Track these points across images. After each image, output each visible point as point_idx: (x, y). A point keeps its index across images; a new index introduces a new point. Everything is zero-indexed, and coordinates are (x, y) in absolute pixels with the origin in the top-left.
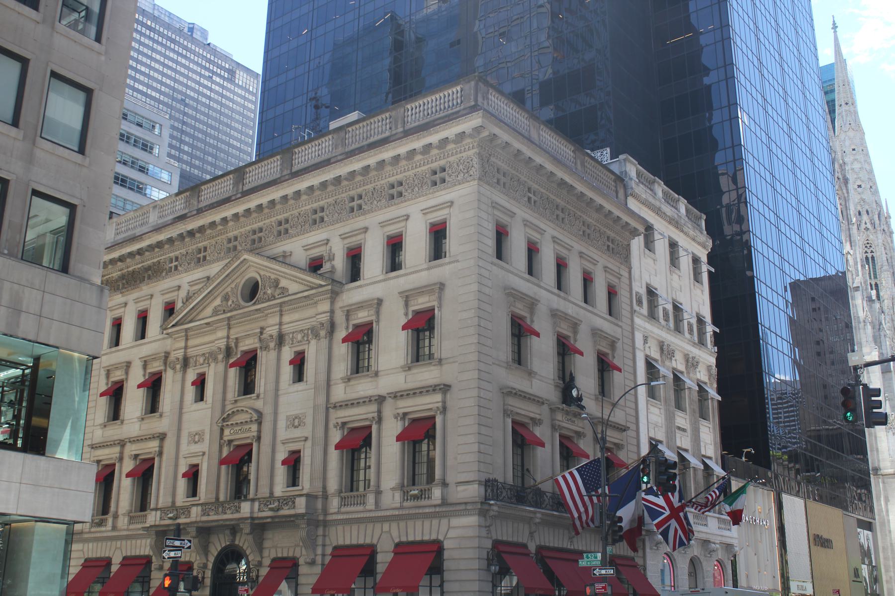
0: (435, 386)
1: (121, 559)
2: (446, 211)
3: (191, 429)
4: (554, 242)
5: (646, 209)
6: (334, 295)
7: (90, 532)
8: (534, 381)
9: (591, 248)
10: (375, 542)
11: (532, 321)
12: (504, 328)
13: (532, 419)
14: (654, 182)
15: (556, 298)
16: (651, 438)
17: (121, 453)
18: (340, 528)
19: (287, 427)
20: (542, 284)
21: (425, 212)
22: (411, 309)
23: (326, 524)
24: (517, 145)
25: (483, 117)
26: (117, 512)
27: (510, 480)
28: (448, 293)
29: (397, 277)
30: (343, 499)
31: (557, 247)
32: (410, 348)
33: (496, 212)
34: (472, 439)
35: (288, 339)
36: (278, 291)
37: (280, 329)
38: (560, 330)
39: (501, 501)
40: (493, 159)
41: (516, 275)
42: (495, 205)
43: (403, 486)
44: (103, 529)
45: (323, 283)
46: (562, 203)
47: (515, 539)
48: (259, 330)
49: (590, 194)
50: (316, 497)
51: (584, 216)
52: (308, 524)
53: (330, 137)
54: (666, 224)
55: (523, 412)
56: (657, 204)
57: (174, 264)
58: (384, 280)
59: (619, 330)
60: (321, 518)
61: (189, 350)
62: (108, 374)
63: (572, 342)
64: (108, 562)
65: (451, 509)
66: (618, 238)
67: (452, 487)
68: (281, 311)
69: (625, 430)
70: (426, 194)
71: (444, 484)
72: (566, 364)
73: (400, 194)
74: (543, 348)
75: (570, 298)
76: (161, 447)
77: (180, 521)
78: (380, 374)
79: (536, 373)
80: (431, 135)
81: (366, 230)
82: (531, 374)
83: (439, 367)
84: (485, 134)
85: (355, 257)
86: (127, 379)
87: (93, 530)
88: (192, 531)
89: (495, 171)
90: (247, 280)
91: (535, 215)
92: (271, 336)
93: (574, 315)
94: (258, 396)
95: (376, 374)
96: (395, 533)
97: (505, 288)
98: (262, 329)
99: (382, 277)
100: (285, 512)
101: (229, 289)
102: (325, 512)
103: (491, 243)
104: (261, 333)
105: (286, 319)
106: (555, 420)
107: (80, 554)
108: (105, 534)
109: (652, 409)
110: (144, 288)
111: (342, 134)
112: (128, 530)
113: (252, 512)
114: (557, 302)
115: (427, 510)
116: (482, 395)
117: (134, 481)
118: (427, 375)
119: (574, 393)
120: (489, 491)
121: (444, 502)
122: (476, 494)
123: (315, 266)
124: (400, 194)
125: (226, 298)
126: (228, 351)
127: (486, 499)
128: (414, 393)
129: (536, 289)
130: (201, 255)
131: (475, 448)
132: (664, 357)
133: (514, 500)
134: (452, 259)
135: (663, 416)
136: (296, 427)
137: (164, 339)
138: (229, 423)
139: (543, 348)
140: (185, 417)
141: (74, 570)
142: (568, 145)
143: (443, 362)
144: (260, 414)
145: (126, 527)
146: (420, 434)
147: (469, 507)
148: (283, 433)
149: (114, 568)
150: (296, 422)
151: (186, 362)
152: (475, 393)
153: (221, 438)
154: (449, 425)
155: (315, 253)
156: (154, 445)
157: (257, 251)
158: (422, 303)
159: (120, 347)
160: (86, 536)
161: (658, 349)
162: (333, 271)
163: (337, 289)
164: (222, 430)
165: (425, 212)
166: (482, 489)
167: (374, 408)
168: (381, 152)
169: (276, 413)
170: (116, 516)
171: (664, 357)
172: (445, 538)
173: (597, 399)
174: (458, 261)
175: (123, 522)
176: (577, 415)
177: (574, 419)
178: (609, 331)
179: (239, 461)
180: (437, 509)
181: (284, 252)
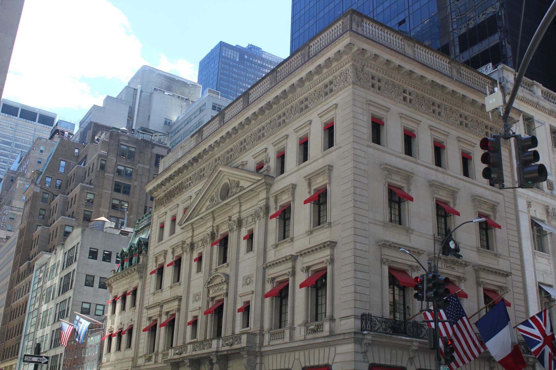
0: (324, 243)
2: (333, 112)
3: (193, 292)
4: (431, 129)
5: (525, 105)
6: (269, 186)
7: (144, 365)
8: (413, 237)
9: (468, 134)
10: (290, 367)
11: (409, 190)
12: (382, 196)
13: (410, 266)
14: (533, 85)
15: (434, 172)
16: (539, 283)
17: (161, 311)
18: (270, 357)
19: (243, 285)
20: (419, 161)
21: (320, 116)
22: (313, 188)
23: (262, 355)
24: (385, 55)
25: (350, 36)
27: (387, 314)
28: (335, 173)
29: (305, 166)
30: (272, 335)
31: (433, 133)
32: (312, 217)
33: (371, 108)
34: (350, 282)
35: (244, 222)
36: (239, 189)
37: (239, 216)
38: (439, 197)
39: (375, 331)
40: (367, 69)
41: (392, 155)
42: (370, 103)
43: (307, 322)
45: (260, 178)
46: (438, 101)
47: (393, 363)
48: (228, 218)
49: (461, 91)
50: (255, 334)
51: (461, 110)
52: (248, 355)
53: (268, 78)
54: (547, 116)
55: (399, 261)
56: (536, 100)
57: (189, 182)
58: (297, 170)
59: (501, 197)
60: (257, 350)
61: (194, 238)
63: (452, 206)
65: (335, 339)
66: (496, 126)
67: (337, 321)
68: (240, 203)
69: (507, 276)
70: (321, 103)
71: (332, 319)
72: (448, 224)
73: (307, 107)
74: (421, 212)
75: (448, 172)
76: (179, 305)
77: (182, 355)
78: (294, 239)
79: (413, 230)
80: (320, 58)
81: (287, 136)
82: (409, 231)
83: (329, 229)
84: (355, 49)
85: (281, 157)
88: (187, 362)
89: (368, 78)
90: (223, 185)
91: (412, 109)
92: (234, 221)
93: (453, 185)
94: (228, 265)
95: (292, 240)
96: (302, 360)
97: (381, 165)
98: (230, 217)
99: (296, 169)
100: (236, 346)
101: (214, 193)
102: (261, 345)
103: (366, 131)
104: (230, 220)
105: (243, 208)
106: (480, 278)
109: (540, 259)
110: (175, 201)
111: (275, 74)
113: (218, 347)
114: (436, 175)
115: (320, 341)
116: (358, 247)
118: (323, 235)
119: (452, 245)
120: (364, 323)
121: (332, 333)
122: (353, 327)
123: (260, 167)
124: (307, 107)
125: (212, 200)
126: (213, 235)
127: (362, 330)
128: (312, 251)
129: (413, 165)
130: (202, 174)
131: (352, 289)
132: (550, 218)
133: (389, 330)
134: (337, 147)
135: (552, 266)
136: (248, 284)
137: (183, 232)
138: (213, 284)
139: (421, 212)
140: (192, 284)
142: (443, 58)
143: (332, 225)
144: (227, 276)
146: (318, 283)
147: (347, 337)
148: (241, 290)
150: (247, 281)
151: (192, 246)
152: (352, 246)
153: (208, 296)
154: (336, 273)
155: (259, 159)
156: (175, 304)
157: (229, 165)
158: (319, 183)
159: (163, 241)
161: (544, 212)
162: (268, 170)
163: (269, 181)
164: (209, 291)
165: (320, 116)
166: (359, 322)
167: (289, 265)
168: (291, 79)
169: (237, 276)
170: (157, 355)
171: (550, 218)
172: (333, 363)
173: (478, 251)
174: (341, 147)
176: (453, 262)
177: (454, 266)
178: (490, 198)
179: (218, 311)
180: (327, 340)
181: (243, 162)
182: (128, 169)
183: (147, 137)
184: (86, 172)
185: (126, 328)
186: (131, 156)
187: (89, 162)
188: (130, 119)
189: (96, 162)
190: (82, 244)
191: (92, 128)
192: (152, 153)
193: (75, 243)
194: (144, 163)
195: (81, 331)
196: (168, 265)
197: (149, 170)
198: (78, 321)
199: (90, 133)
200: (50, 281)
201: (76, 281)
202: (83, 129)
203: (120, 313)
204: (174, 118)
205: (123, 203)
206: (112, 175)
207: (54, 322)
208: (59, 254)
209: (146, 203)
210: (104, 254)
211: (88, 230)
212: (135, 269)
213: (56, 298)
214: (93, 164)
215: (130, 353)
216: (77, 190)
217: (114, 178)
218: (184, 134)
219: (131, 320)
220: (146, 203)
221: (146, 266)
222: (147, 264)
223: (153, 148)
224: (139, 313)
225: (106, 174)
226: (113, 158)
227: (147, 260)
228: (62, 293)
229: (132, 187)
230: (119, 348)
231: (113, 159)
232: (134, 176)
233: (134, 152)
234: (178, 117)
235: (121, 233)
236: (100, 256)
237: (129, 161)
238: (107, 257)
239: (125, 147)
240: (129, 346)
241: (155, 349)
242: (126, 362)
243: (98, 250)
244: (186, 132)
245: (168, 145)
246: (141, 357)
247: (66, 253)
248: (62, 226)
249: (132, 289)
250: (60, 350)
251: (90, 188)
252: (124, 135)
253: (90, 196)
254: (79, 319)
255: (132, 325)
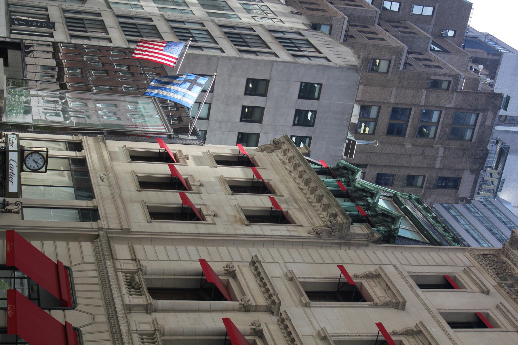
1: (74, 325)
7: (116, 270)
17: (256, 309)
26: (156, 310)
44: (125, 290)
62: (375, 276)
64: (67, 303)
86: (376, 305)
87: (120, 275)
107: (76, 259)
108: (116, 294)
112: (130, 332)
117: (220, 334)
141: (49, 249)
145: (133, 327)
149: (57, 315)
160: (109, 264)
175: (142, 322)
182: (433, 129)
183: (492, 160)
184: (420, 54)
185: (193, 198)
186: (456, 133)
187: (442, 59)
188: (502, 119)
189: (445, 71)
190: (331, 67)
191: (490, 57)
192: (463, 170)
193: (326, 52)
194: (444, 157)
195: (176, 92)
196: (380, 325)
197: (432, 167)
198: (193, 83)
199: (482, 54)
200: (240, 6)
201: (257, 61)
202: (483, 40)
203: (223, 180)
204: (504, 195)
205: (372, 124)
206: (422, 103)
207: (168, 21)
208: (294, 20)
209: (371, 165)
210: (307, 112)
211: (356, 77)
212: (335, 216)
213: (212, 21)
214: (438, 67)
215: (139, 221)
216: (393, 42)
217: (418, 105)
218: (484, 216)
219: (215, 215)
220: (371, 165)
221: (345, 244)
222: (349, 245)
223: (472, 171)
224: (236, 235)
225: (425, 92)
226: (453, 102)
227: (359, 246)
228: (226, 33)
229: (400, 139)
230: (146, 184)
231: (451, 101)
232: (422, 141)
233: (462, 138)
234: (509, 203)
235: (350, 140)
236: (306, 104)
237: (447, 130)
238: (301, 119)
239: (472, 122)
240: (157, 214)
241: (161, 303)
242: (117, 208)
243: (318, 99)
244: (489, 221)
245: (477, 199)
246: (133, 252)
247: (300, 34)
248: (330, 18)
249: (283, 207)
250: (118, 39)
251: (399, 64)
252: (494, 119)
253: (383, 66)
254: (200, 85)
255: (204, 219)
